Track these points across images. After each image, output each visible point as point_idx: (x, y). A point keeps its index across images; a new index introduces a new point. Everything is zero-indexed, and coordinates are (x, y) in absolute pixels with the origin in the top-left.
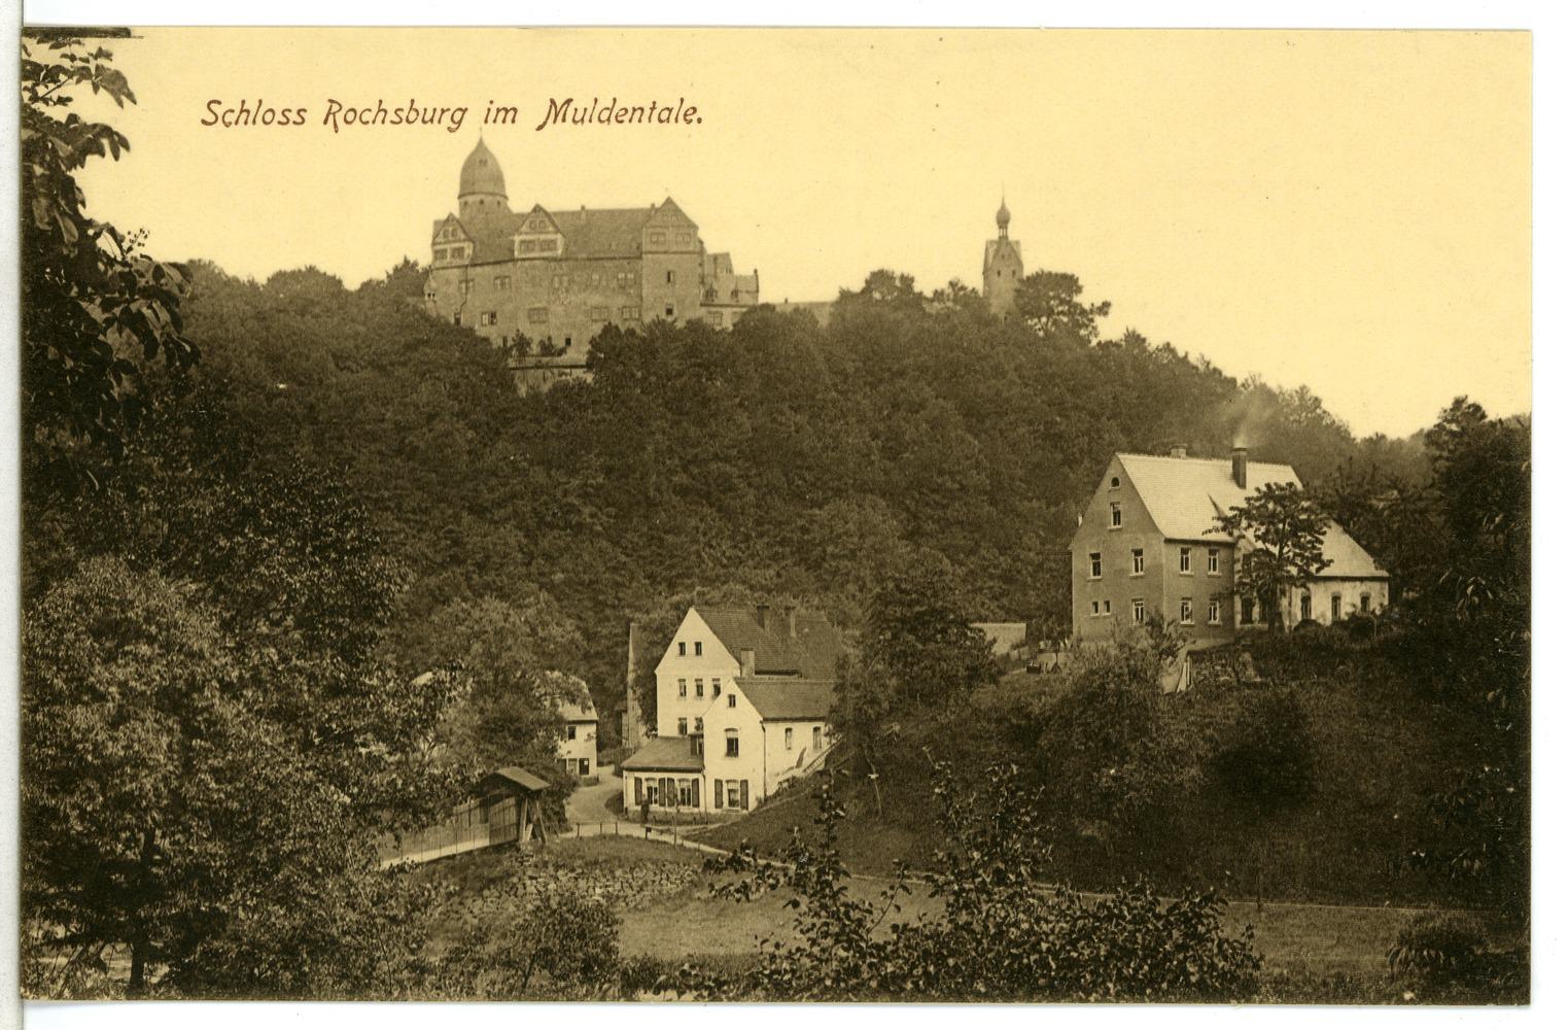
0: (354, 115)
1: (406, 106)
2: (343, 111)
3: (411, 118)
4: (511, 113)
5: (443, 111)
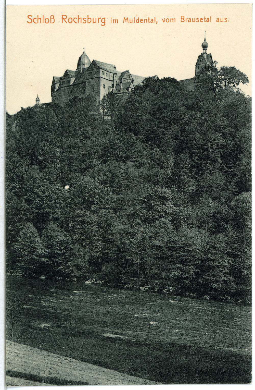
0: (71, 20)
1: (87, 17)
2: (68, 18)
3: (89, 21)
5: (99, 19)
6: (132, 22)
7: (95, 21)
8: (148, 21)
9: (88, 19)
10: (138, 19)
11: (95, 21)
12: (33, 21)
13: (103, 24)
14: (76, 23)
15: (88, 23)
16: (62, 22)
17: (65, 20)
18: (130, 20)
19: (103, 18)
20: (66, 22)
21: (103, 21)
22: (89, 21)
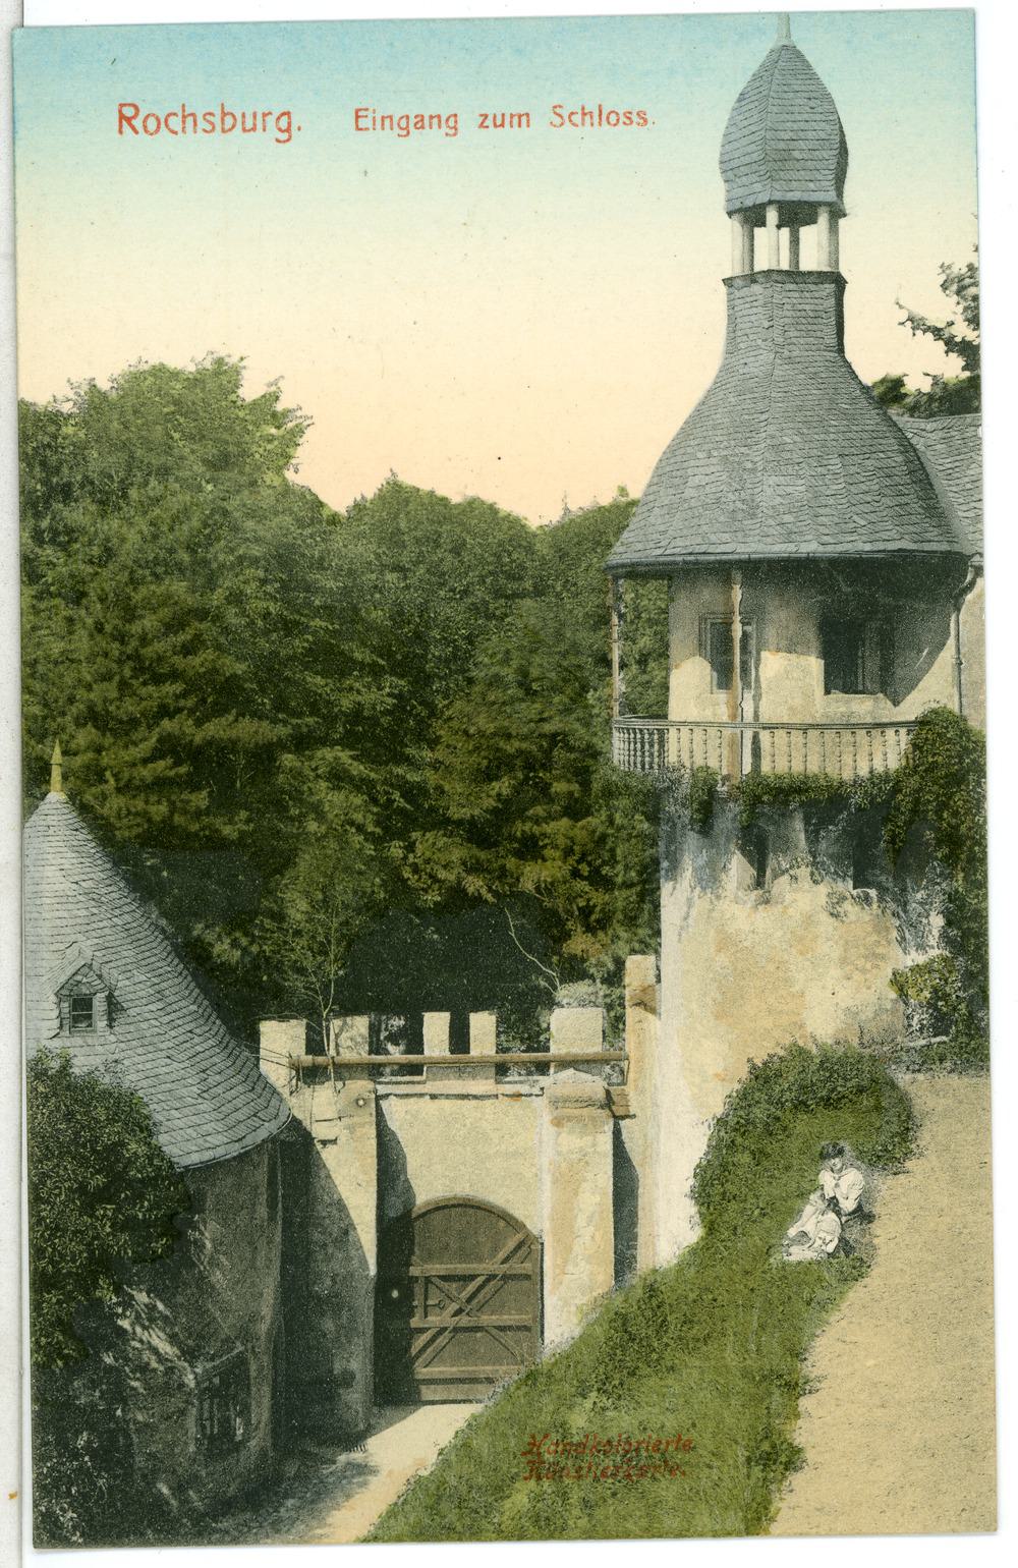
1: (218, 112)
3: (228, 125)
4: (524, 119)
6: (502, 125)
7: (249, 125)
8: (490, 118)
9: (224, 114)
12: (163, 125)
13: (284, 136)
14: (175, 133)
15: (223, 131)
16: (121, 132)
17: (134, 122)
19: (283, 114)
20: (136, 132)
21: (283, 123)
22: (228, 125)
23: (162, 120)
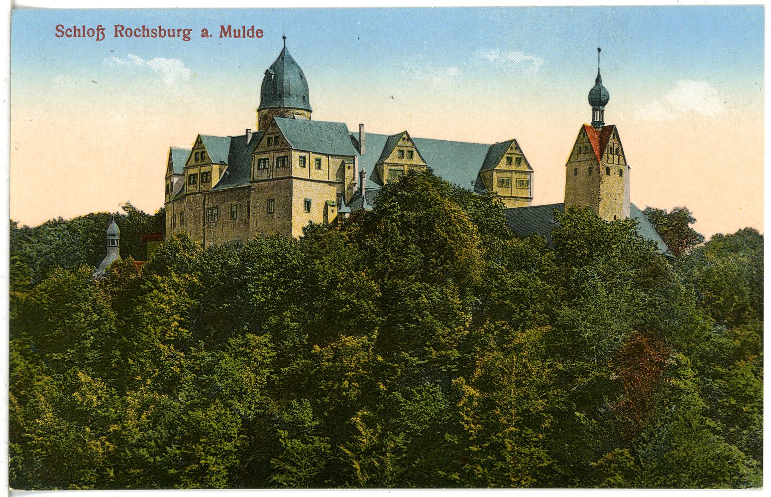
0: (131, 33)
1: (158, 29)
2: (125, 30)
3: (163, 35)
9: (160, 30)
10: (253, 30)
11: (171, 34)
15: (160, 35)
18: (235, 31)
20: (122, 36)
23: (133, 33)
